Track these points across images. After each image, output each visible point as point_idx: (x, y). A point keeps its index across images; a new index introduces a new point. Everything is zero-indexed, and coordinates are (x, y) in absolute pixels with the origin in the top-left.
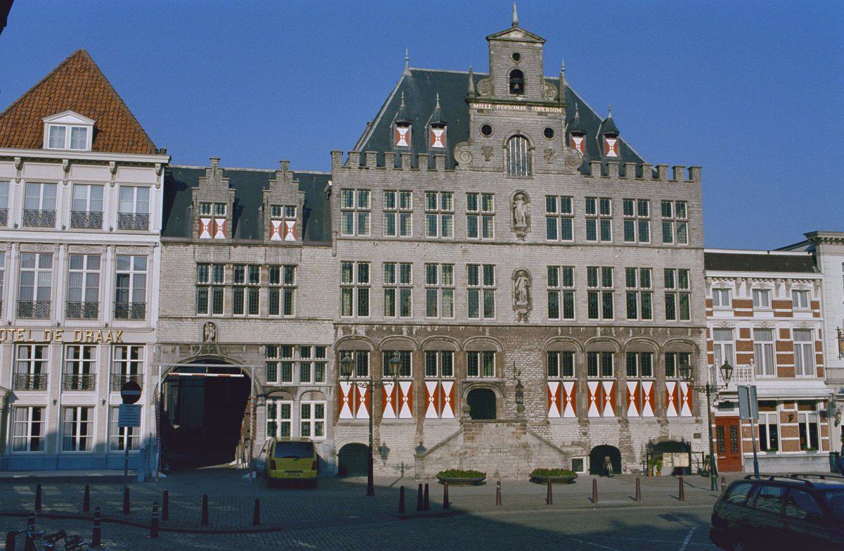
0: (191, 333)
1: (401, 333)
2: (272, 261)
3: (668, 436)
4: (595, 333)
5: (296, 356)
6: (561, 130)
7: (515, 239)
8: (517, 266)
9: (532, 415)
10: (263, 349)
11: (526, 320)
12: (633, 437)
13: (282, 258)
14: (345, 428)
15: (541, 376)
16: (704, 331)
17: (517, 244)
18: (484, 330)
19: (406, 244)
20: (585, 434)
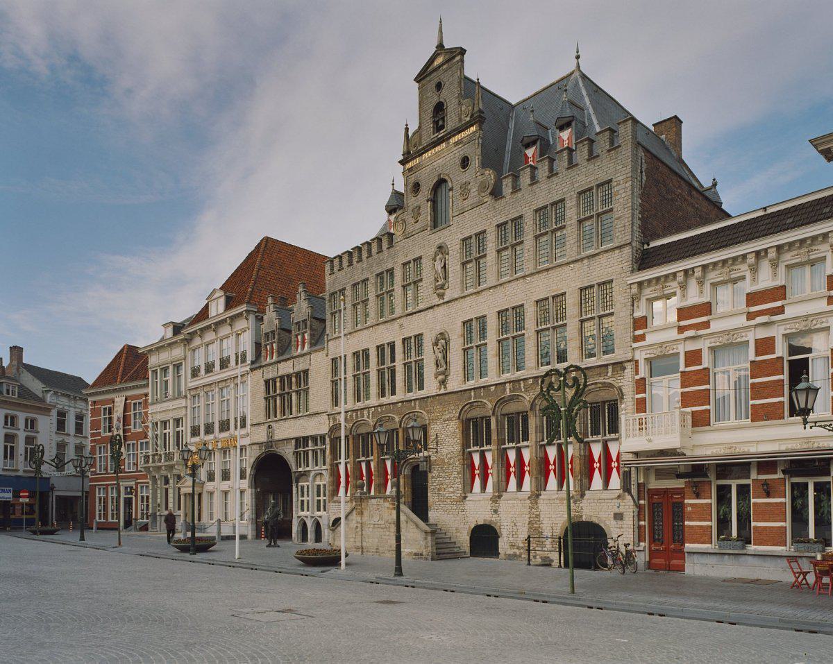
0: (261, 435)
1: (363, 417)
2: (296, 369)
3: (581, 516)
4: (505, 390)
5: (311, 446)
6: (475, 162)
7: (437, 301)
8: (438, 329)
9: (451, 490)
10: (293, 441)
11: (445, 387)
12: (542, 516)
13: (300, 365)
14: (334, 504)
15: (458, 447)
16: (629, 366)
17: (438, 305)
18: (415, 404)
19: (365, 331)
20: (495, 511)
